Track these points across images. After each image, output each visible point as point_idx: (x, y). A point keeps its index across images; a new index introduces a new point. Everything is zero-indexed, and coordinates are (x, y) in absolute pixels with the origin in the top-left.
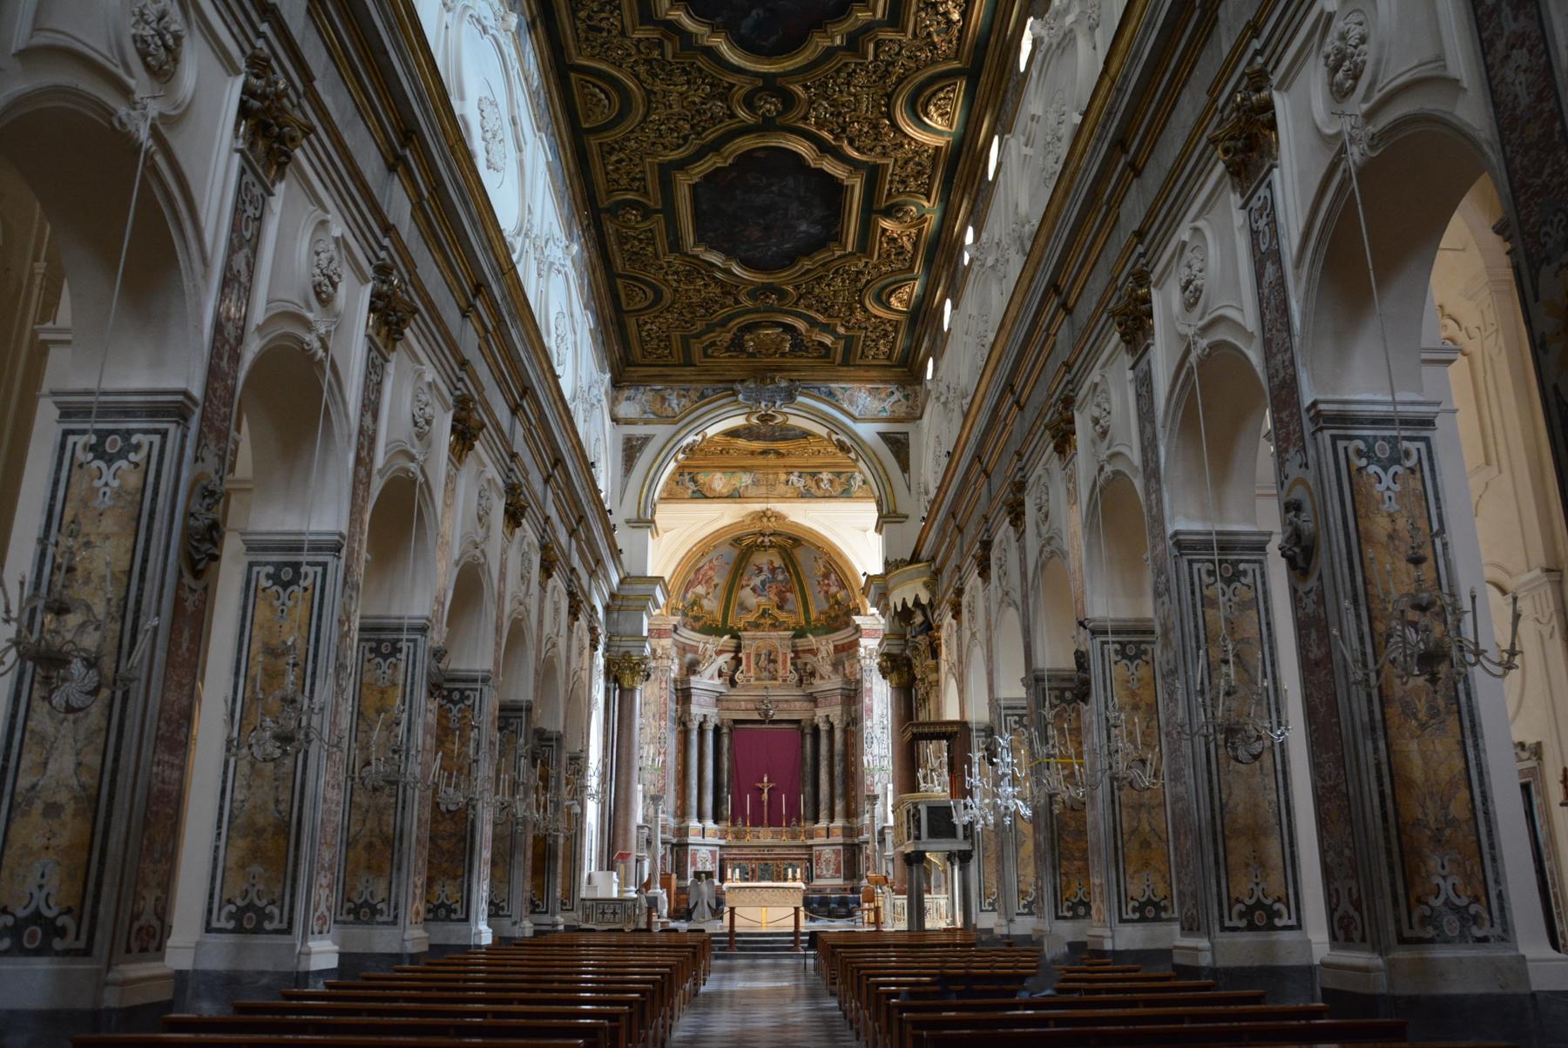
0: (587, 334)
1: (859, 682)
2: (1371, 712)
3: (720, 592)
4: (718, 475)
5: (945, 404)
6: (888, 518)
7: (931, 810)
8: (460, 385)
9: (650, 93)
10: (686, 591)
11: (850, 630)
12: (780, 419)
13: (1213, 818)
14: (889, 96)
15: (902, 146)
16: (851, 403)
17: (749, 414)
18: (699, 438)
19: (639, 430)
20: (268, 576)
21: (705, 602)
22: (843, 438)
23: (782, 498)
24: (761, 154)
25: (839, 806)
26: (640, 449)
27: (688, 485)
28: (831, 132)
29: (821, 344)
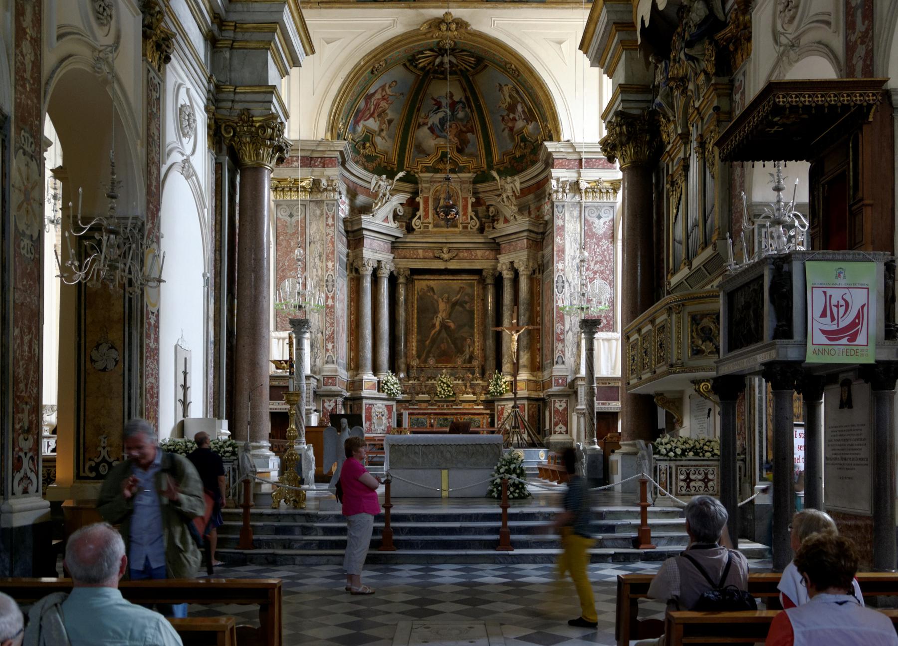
10: (356, 123)
11: (539, 166)
21: (378, 140)
25: (524, 359)
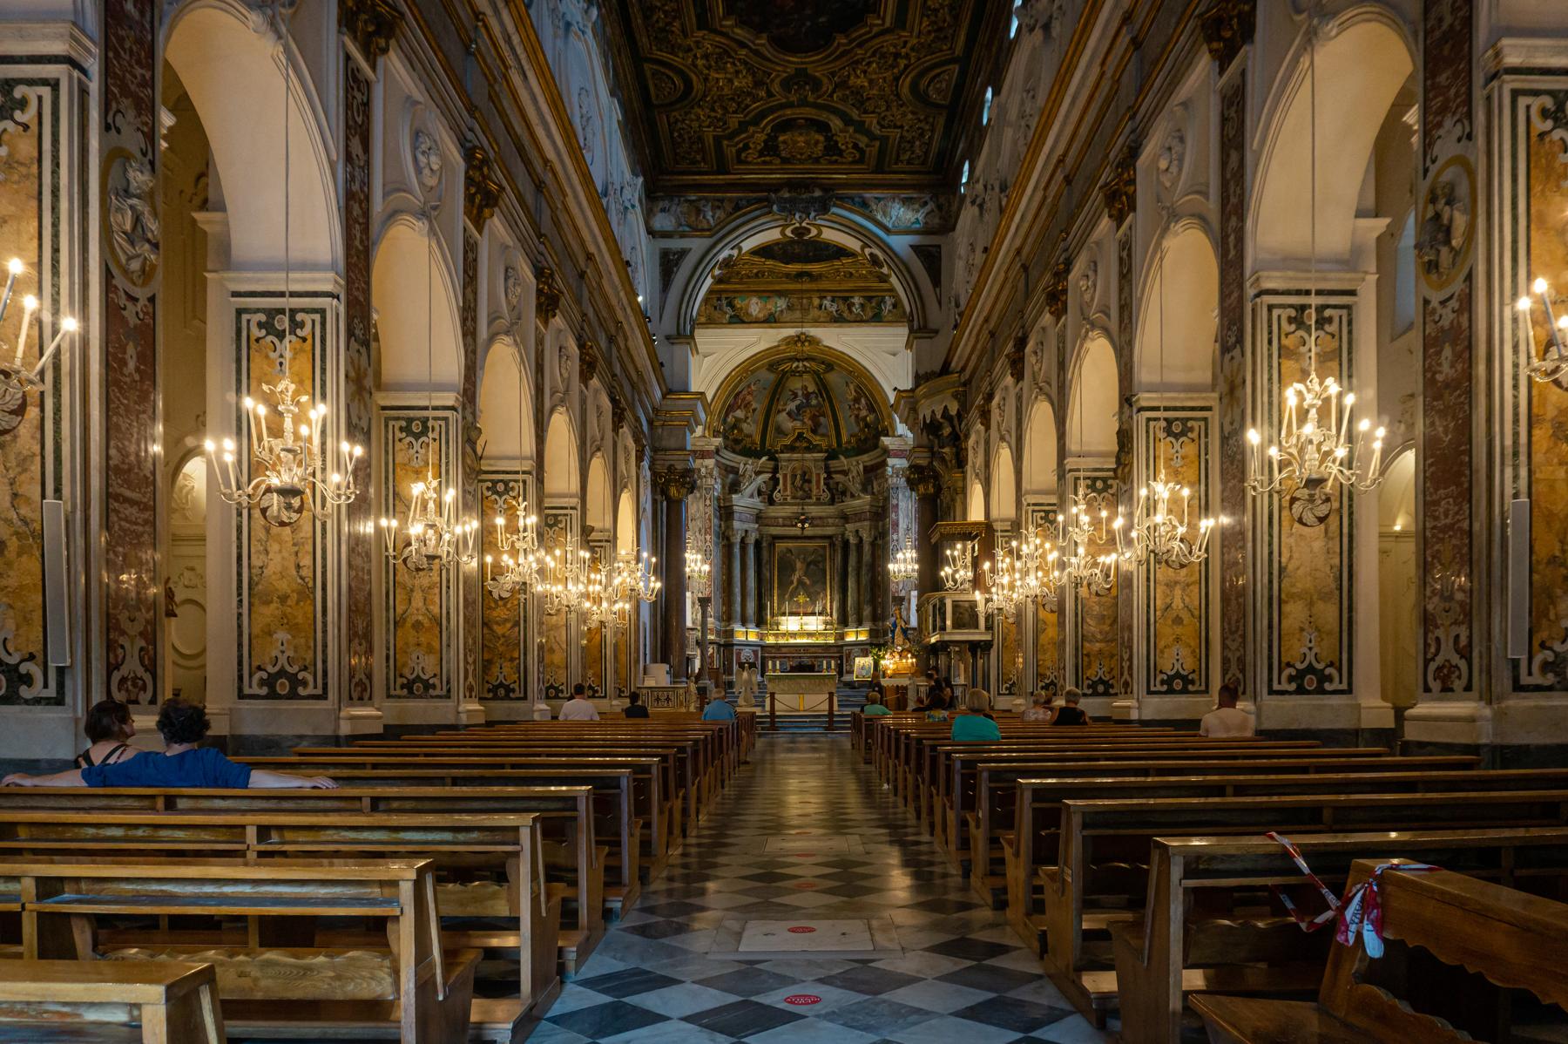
0: (615, 126)
1: (887, 499)
2: (1516, 434)
3: (760, 416)
4: (754, 300)
5: (981, 206)
6: (921, 330)
7: (956, 605)
8: (470, 135)
10: (727, 415)
12: (814, 232)
13: (1271, 582)
16: (885, 214)
17: (785, 227)
18: (735, 252)
19: (676, 244)
20: (260, 325)
21: (744, 426)
22: (877, 252)
23: (816, 322)
25: (867, 611)
26: (677, 263)
27: (726, 309)
29: (856, 146)
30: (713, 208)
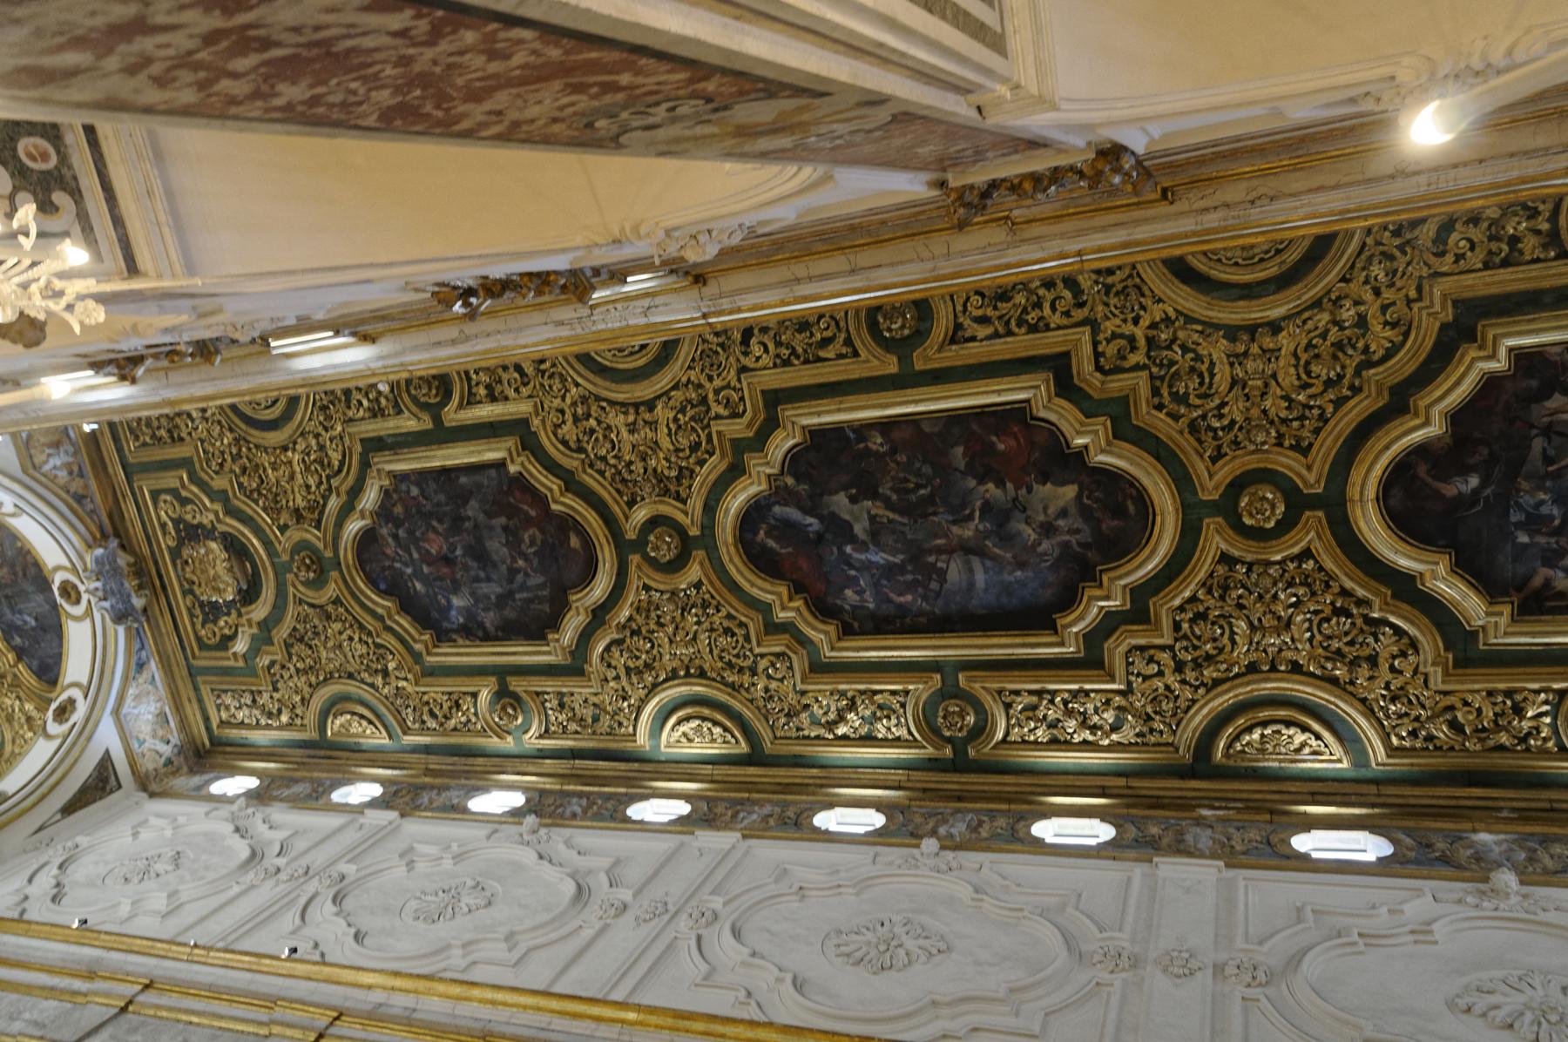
9: (650, 405)
14: (702, 674)
15: (624, 699)
16: (137, 697)
22: (82, 708)
24: (574, 542)
28: (631, 618)
30: (68, 466)
